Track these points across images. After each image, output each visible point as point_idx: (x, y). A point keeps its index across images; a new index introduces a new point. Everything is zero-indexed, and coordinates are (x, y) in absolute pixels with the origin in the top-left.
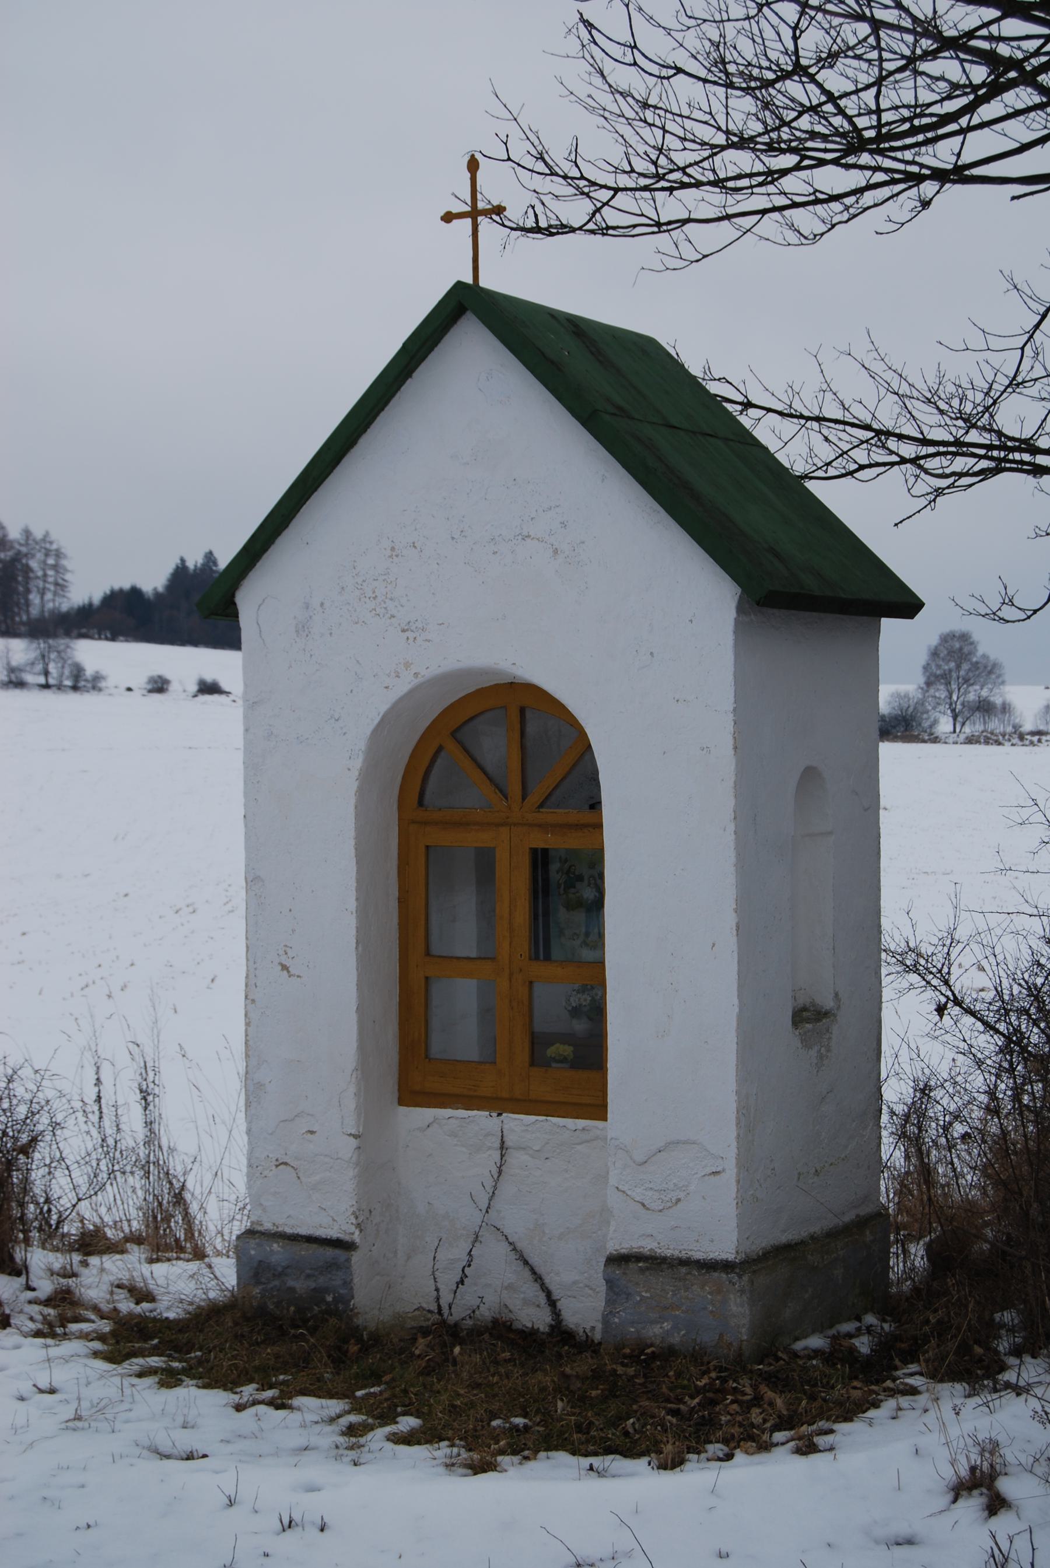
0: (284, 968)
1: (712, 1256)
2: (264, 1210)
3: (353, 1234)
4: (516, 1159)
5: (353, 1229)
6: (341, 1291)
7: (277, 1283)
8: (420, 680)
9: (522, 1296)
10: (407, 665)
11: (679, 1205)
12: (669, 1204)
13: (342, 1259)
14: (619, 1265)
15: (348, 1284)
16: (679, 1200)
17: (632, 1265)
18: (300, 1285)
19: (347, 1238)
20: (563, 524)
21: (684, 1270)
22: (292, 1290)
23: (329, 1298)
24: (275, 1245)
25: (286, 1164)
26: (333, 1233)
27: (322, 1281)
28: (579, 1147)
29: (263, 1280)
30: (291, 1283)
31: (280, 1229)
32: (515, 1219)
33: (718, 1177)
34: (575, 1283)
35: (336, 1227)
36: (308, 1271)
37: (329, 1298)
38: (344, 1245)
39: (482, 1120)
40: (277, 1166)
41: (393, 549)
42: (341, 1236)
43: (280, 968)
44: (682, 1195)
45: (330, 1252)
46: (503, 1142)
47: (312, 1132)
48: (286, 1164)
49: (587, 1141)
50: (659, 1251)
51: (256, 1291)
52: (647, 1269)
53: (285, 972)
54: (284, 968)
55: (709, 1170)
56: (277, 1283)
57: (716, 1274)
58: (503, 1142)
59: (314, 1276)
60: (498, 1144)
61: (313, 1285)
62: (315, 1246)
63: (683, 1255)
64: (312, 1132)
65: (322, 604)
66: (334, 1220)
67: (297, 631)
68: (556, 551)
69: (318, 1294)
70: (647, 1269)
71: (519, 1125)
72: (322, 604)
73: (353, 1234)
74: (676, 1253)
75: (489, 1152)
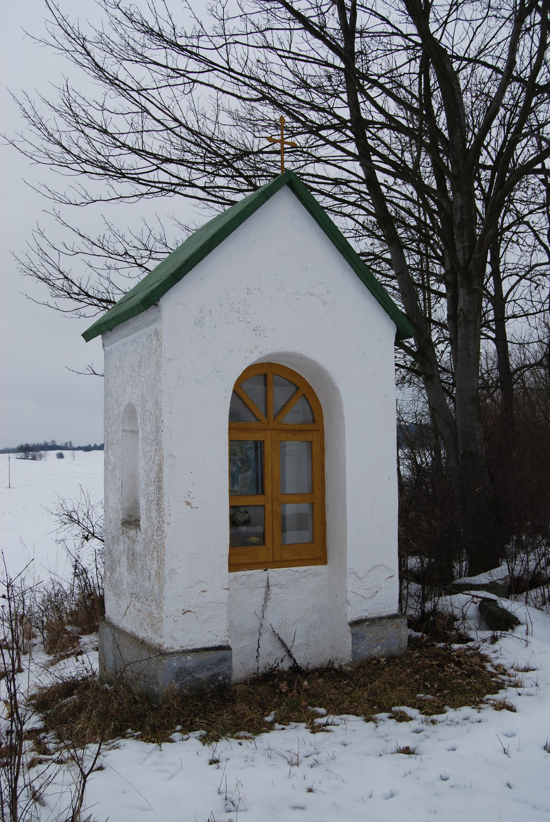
0: (188, 503)
1: (389, 613)
2: (175, 640)
3: (228, 641)
4: (273, 589)
5: (228, 638)
6: (227, 673)
7: (188, 678)
8: (262, 355)
9: (275, 657)
10: (256, 347)
11: (378, 593)
12: (373, 594)
13: (228, 655)
14: (359, 626)
15: (230, 668)
16: (377, 592)
17: (364, 624)
18: (203, 676)
19: (225, 644)
20: (328, 292)
21: (384, 621)
22: (199, 679)
23: (220, 678)
24: (189, 657)
25: (189, 611)
26: (217, 643)
27: (216, 670)
28: (302, 580)
29: (180, 678)
30: (197, 676)
31: (184, 648)
32: (273, 619)
33: (392, 578)
34: (301, 644)
35: (218, 640)
36: (208, 667)
37: (220, 678)
38: (227, 648)
39: (258, 574)
40: (184, 614)
41: (248, 289)
42: (221, 644)
43: (186, 504)
44: (378, 589)
45: (221, 653)
46: (268, 583)
47: (204, 591)
48: (189, 611)
49: (306, 576)
50: (369, 616)
51: (176, 686)
52: (370, 624)
53: (189, 506)
54: (188, 503)
55: (387, 576)
56: (188, 678)
57: (396, 620)
58: (268, 583)
59: (212, 668)
60: (266, 584)
61: (210, 673)
62: (212, 652)
63: (378, 616)
64: (204, 591)
65: (210, 312)
66: (217, 636)
67: (196, 324)
68: (325, 303)
69: (213, 678)
70: (370, 624)
71: (277, 574)
72: (210, 312)
73: (228, 641)
74: (376, 615)
75: (259, 590)
